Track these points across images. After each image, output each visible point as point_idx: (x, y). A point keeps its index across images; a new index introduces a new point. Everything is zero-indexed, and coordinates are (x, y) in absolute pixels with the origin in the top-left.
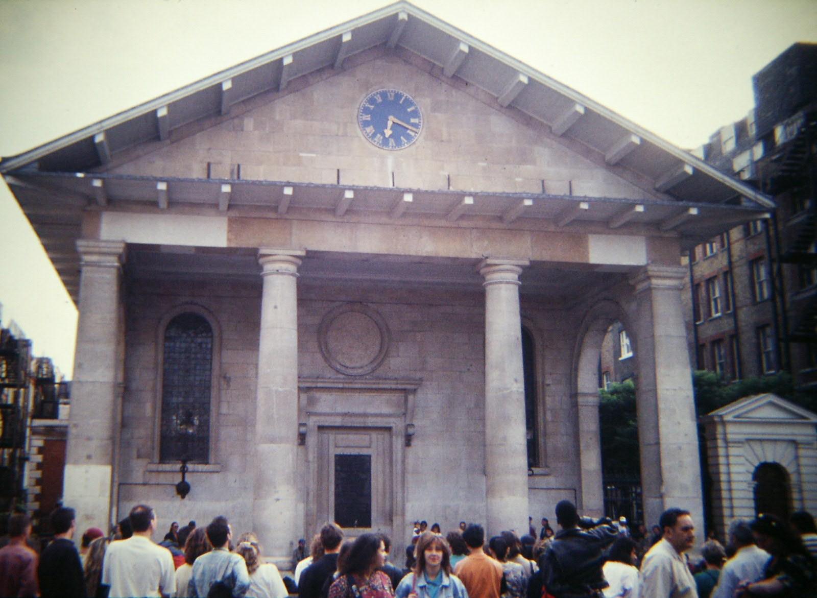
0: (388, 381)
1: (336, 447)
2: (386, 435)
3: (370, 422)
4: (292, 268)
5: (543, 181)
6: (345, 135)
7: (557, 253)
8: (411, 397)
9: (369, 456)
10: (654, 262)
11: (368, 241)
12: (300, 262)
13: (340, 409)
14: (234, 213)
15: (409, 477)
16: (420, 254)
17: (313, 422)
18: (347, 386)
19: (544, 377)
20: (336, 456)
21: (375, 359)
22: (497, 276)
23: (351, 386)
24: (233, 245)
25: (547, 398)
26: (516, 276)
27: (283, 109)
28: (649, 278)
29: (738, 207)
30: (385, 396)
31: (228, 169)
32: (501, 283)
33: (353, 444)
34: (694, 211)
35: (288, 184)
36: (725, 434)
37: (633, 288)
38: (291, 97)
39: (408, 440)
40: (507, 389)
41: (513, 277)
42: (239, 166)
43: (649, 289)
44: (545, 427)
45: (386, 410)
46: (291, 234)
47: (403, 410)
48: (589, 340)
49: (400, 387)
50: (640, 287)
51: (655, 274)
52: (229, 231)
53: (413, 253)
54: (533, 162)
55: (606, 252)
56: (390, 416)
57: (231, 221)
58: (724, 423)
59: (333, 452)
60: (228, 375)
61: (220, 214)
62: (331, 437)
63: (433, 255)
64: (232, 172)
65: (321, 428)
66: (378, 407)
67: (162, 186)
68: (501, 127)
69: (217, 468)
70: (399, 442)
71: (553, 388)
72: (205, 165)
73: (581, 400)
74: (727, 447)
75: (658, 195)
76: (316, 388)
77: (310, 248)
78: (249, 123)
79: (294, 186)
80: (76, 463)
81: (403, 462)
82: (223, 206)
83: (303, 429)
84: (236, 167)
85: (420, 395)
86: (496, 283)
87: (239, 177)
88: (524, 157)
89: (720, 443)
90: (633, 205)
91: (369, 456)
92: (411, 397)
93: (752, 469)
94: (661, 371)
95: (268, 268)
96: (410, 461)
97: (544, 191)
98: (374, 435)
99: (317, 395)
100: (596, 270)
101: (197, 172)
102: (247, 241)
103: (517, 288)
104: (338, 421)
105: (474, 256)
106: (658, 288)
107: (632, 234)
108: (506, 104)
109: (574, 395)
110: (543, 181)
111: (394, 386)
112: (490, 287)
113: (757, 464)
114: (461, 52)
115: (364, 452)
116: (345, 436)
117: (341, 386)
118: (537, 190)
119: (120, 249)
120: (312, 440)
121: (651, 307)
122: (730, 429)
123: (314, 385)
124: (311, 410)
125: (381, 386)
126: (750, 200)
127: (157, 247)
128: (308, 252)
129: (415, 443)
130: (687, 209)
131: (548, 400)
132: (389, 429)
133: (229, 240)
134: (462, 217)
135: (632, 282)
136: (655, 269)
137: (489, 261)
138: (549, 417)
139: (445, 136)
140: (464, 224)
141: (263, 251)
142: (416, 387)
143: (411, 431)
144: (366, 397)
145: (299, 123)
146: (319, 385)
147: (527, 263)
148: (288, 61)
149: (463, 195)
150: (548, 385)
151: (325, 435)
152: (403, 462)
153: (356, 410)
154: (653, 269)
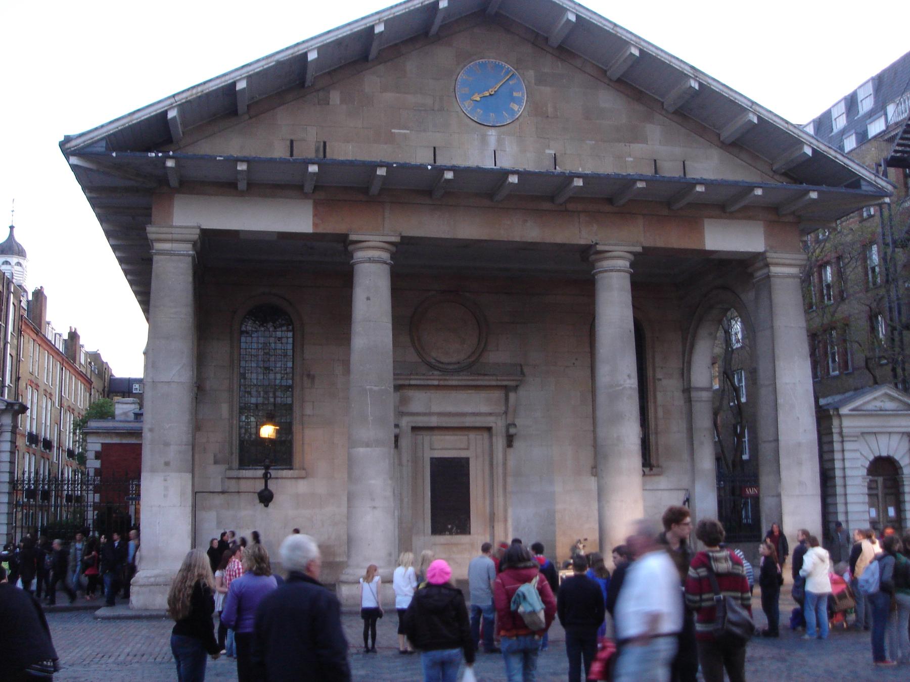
0: (486, 378)
1: (431, 449)
2: (486, 435)
3: (469, 421)
4: (385, 256)
5: (655, 161)
6: (441, 109)
7: (673, 238)
8: (512, 396)
9: (467, 460)
11: (467, 228)
12: (394, 249)
13: (435, 408)
15: (510, 480)
16: (524, 240)
17: (405, 422)
18: (442, 383)
19: (654, 371)
20: (432, 459)
21: (473, 353)
22: (606, 264)
23: (446, 383)
24: (321, 230)
26: (628, 264)
27: (372, 81)
28: (767, 265)
29: (857, 191)
30: (483, 394)
31: (313, 148)
32: (612, 271)
33: (447, 447)
34: (814, 195)
35: (381, 165)
36: (841, 428)
37: (751, 275)
38: (381, 68)
39: (510, 440)
40: (621, 385)
41: (624, 264)
42: (325, 143)
43: (768, 277)
44: (656, 425)
45: (484, 409)
46: (384, 218)
47: (504, 408)
48: (703, 332)
49: (499, 383)
50: (759, 274)
52: (315, 215)
53: (518, 239)
54: (644, 140)
55: (723, 238)
56: (490, 414)
57: (317, 205)
58: (839, 416)
59: (429, 454)
60: (312, 373)
61: (306, 196)
62: (425, 438)
63: (538, 240)
64: (317, 150)
65: (414, 429)
66: (476, 405)
67: (242, 167)
68: (609, 101)
69: (303, 473)
70: (499, 443)
71: (665, 382)
72: (288, 143)
73: (694, 394)
74: (842, 442)
75: (777, 177)
76: (410, 385)
77: (404, 234)
78: (335, 97)
79: (388, 166)
80: (153, 471)
81: (505, 464)
82: (308, 188)
83: (397, 431)
84: (322, 144)
85: (522, 392)
86: (606, 271)
87: (325, 156)
88: (636, 137)
89: (836, 437)
90: (751, 188)
91: (467, 460)
92: (512, 396)
93: (867, 464)
94: (781, 365)
95: (359, 255)
96: (511, 463)
97: (656, 172)
98: (472, 435)
99: (410, 393)
100: (712, 257)
101: (279, 152)
102: (334, 225)
103: (628, 275)
104: (434, 421)
105: (582, 242)
106: (777, 276)
107: (750, 218)
108: (615, 78)
109: (687, 390)
110: (655, 161)
111: (494, 383)
112: (601, 275)
113: (871, 458)
114: (568, 21)
115: (463, 454)
116: (443, 437)
117: (436, 383)
118: (649, 171)
119: (195, 235)
120: (404, 443)
121: (770, 293)
122: (846, 423)
123: (407, 382)
124: (405, 409)
125: (479, 383)
126: (870, 183)
127: (236, 233)
128: (403, 238)
129: (516, 444)
130: (807, 192)
131: (659, 396)
132: (489, 429)
133: (315, 225)
134: (572, 199)
135: (750, 270)
136: (775, 255)
137: (599, 248)
138: (660, 413)
139: (550, 110)
140: (571, 206)
141: (353, 237)
142: (518, 383)
143: (512, 431)
144: (462, 395)
145: (389, 96)
146: (412, 382)
147: (639, 249)
148: (379, 29)
149: (572, 176)
150: (660, 380)
151: (420, 437)
152: (505, 464)
153: (451, 409)
154: (772, 256)
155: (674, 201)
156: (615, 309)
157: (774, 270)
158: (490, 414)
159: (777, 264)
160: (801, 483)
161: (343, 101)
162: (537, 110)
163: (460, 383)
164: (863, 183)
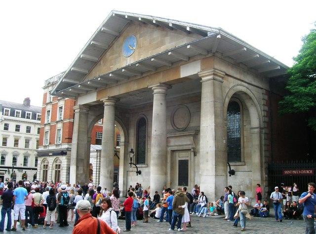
3: (185, 148)
7: (171, 77)
10: (203, 70)
13: (177, 144)
14: (97, 90)
25: (244, 132)
45: (189, 143)
51: (204, 75)
52: (97, 96)
55: (187, 71)
59: (178, 159)
65: (173, 151)
68: (157, 35)
70: (192, 154)
88: (162, 43)
107: (195, 61)
117: (173, 136)
140: (144, 75)
144: (183, 139)
145: (110, 57)
153: (180, 144)
155: (171, 62)
156: (158, 108)
157: (203, 79)
158: (190, 145)
159: (204, 76)
160: (207, 170)
161: (103, 62)
162: (139, 47)
163: (180, 135)
164: (208, 33)
